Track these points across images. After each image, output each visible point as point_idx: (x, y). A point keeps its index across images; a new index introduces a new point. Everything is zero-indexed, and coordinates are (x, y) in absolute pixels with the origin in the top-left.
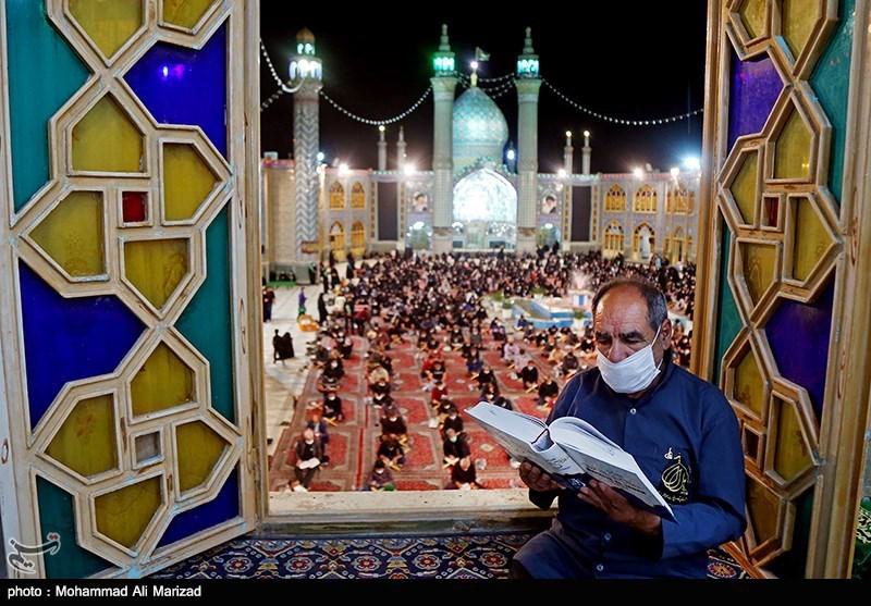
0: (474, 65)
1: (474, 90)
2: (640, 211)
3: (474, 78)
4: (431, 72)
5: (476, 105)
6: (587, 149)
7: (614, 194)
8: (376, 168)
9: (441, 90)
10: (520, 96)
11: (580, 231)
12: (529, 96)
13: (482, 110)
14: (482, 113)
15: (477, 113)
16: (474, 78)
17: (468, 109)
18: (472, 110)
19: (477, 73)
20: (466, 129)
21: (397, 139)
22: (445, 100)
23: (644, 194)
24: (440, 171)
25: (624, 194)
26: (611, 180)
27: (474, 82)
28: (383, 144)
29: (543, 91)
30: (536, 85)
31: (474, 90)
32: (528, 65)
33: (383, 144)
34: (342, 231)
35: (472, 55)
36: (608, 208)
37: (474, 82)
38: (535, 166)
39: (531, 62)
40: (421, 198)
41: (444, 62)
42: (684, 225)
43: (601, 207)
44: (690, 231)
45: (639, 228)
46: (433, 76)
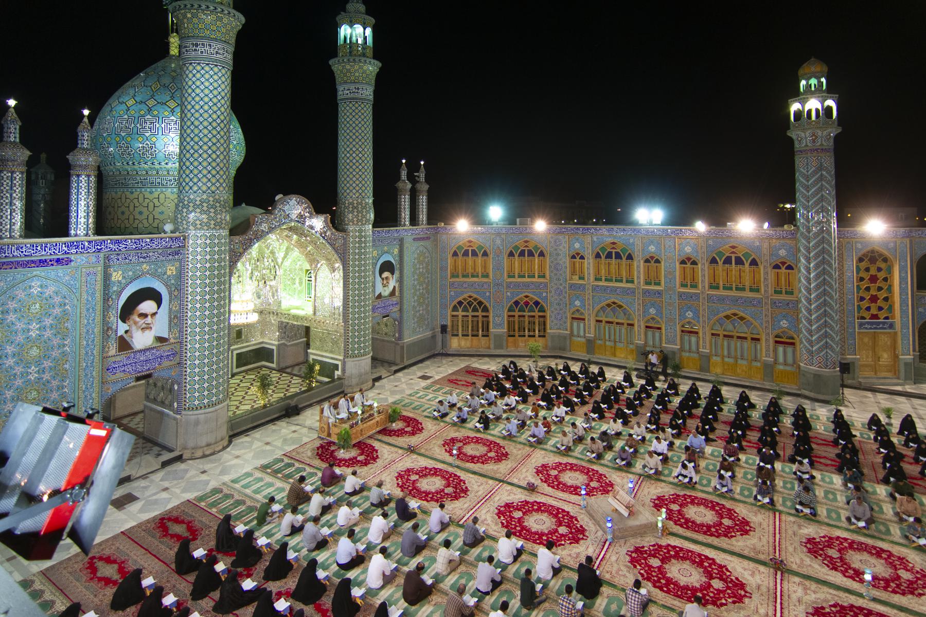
36: (453, 276)
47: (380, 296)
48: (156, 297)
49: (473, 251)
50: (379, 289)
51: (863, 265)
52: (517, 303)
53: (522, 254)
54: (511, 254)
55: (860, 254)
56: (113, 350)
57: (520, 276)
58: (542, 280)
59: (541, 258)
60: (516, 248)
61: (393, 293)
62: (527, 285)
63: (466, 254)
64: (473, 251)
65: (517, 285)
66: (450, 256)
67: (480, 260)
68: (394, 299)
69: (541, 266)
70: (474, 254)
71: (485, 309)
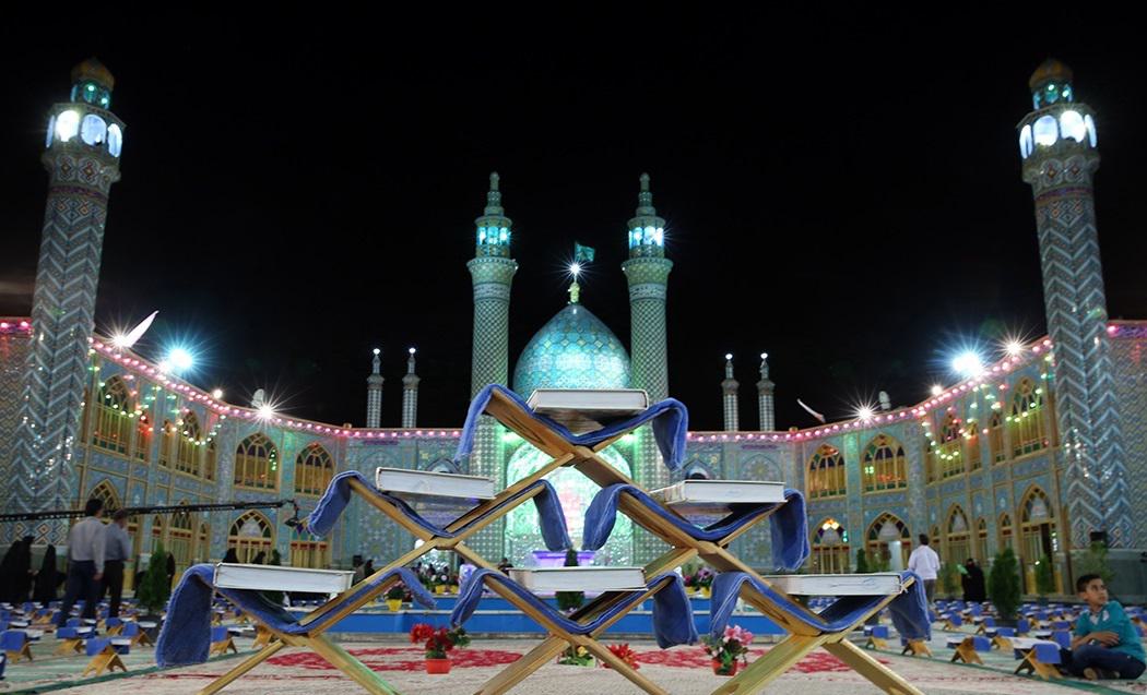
0: (575, 269)
3: (574, 290)
4: (469, 249)
5: (575, 329)
6: (765, 385)
7: (823, 465)
8: (360, 422)
10: (632, 290)
12: (649, 284)
13: (581, 338)
14: (581, 343)
15: (576, 342)
16: (574, 290)
18: (565, 337)
19: (580, 281)
20: (553, 369)
21: (405, 372)
22: (493, 298)
23: (879, 455)
24: (480, 427)
25: (841, 462)
26: (815, 438)
27: (574, 298)
28: (376, 380)
29: (674, 282)
30: (662, 267)
32: (650, 234)
33: (376, 380)
34: (267, 534)
35: (571, 256)
37: (574, 298)
39: (650, 230)
41: (494, 234)
42: (962, 499)
44: (979, 509)
45: (878, 527)
46: (473, 256)
49: (830, 459)
57: (878, 488)
58: (904, 489)
59: (901, 458)
60: (871, 447)
64: (830, 459)
66: (807, 470)
67: (836, 469)
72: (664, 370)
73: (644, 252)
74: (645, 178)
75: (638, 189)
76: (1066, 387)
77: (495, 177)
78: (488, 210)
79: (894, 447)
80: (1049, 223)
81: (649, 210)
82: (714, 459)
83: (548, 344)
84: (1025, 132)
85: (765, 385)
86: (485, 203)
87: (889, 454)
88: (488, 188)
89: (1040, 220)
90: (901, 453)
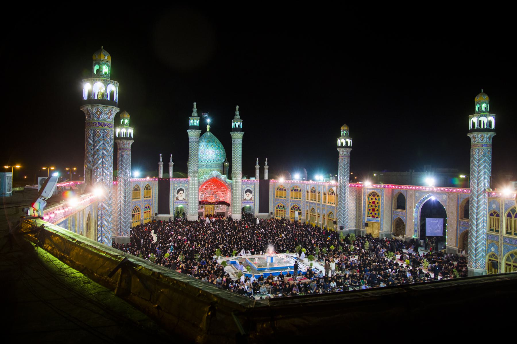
1: (208, 134)
2: (293, 199)
3: (208, 127)
6: (266, 167)
9: (192, 134)
11: (264, 206)
12: (237, 138)
16: (208, 127)
17: (205, 144)
23: (295, 190)
25: (285, 190)
27: (208, 130)
31: (208, 134)
37: (208, 130)
38: (240, 175)
40: (181, 192)
41: (194, 121)
43: (274, 197)
47: (245, 199)
48: (183, 190)
50: (245, 197)
51: (371, 197)
52: (293, 207)
53: (295, 190)
54: (292, 190)
55: (369, 193)
56: (175, 199)
60: (293, 188)
61: (251, 199)
62: (295, 201)
63: (280, 190)
65: (293, 201)
67: (284, 191)
68: (252, 201)
69: (300, 195)
70: (282, 190)
71: (285, 209)
72: (241, 159)
73: (237, 129)
74: (237, 107)
75: (235, 110)
76: (340, 194)
77: (195, 104)
78: (193, 114)
79: (299, 189)
80: (341, 162)
81: (238, 117)
82: (253, 187)
83: (202, 146)
84: (339, 140)
85: (266, 167)
86: (192, 112)
87: (297, 191)
88: (193, 107)
89: (339, 161)
90: (300, 191)
